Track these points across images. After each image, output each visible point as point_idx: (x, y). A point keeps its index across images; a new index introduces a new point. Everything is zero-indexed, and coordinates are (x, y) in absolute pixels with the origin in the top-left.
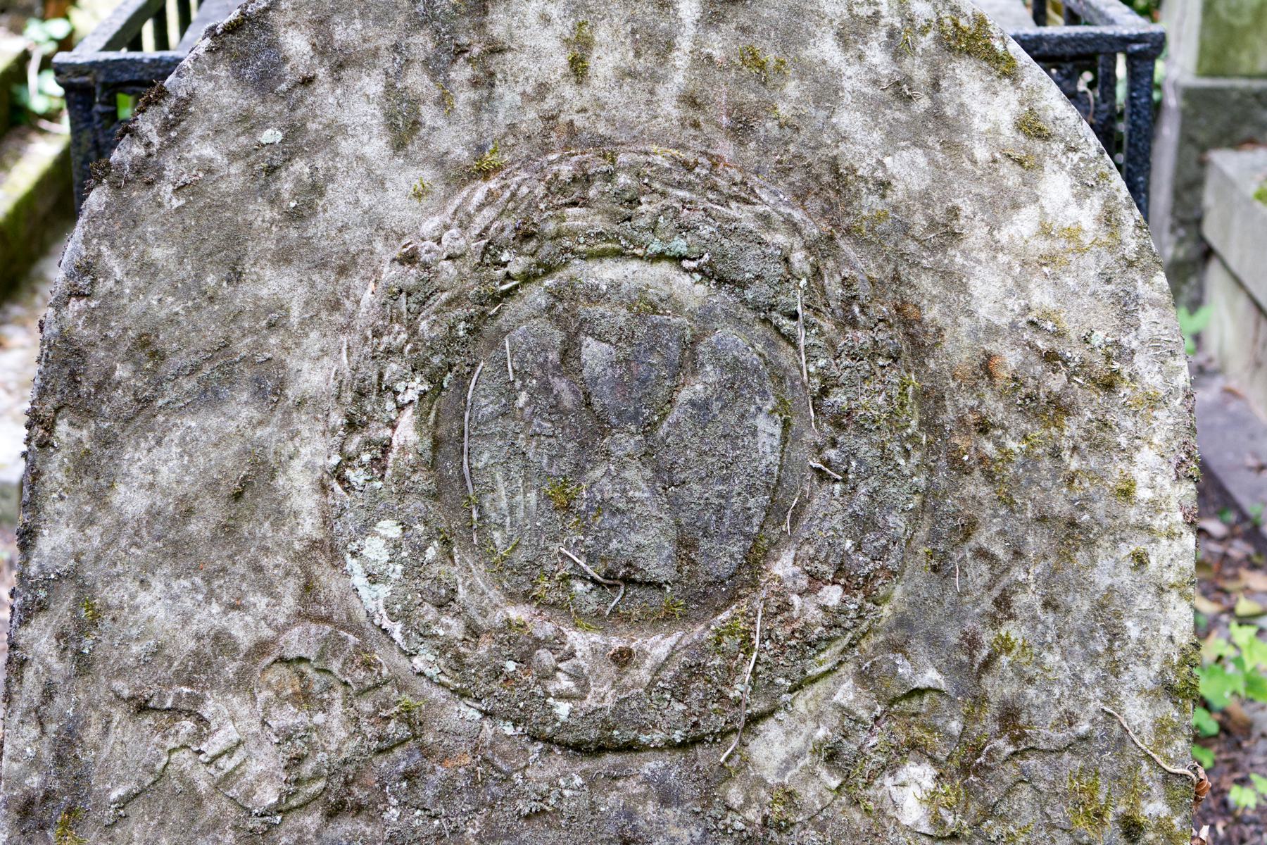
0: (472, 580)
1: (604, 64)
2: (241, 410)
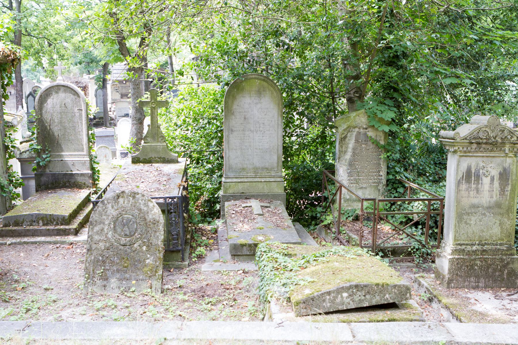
0: (116, 235)
1: (126, 203)
2: (102, 225)
